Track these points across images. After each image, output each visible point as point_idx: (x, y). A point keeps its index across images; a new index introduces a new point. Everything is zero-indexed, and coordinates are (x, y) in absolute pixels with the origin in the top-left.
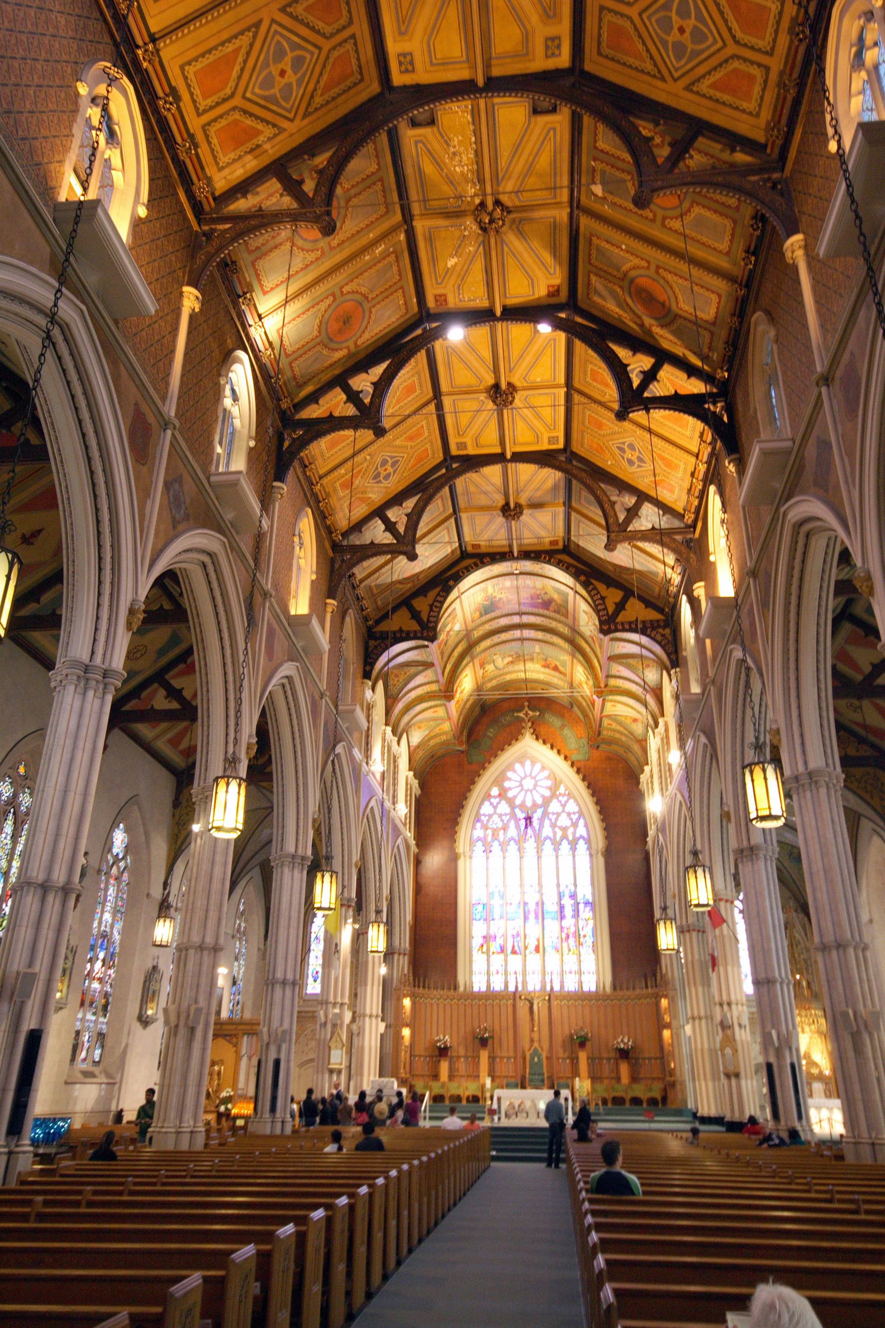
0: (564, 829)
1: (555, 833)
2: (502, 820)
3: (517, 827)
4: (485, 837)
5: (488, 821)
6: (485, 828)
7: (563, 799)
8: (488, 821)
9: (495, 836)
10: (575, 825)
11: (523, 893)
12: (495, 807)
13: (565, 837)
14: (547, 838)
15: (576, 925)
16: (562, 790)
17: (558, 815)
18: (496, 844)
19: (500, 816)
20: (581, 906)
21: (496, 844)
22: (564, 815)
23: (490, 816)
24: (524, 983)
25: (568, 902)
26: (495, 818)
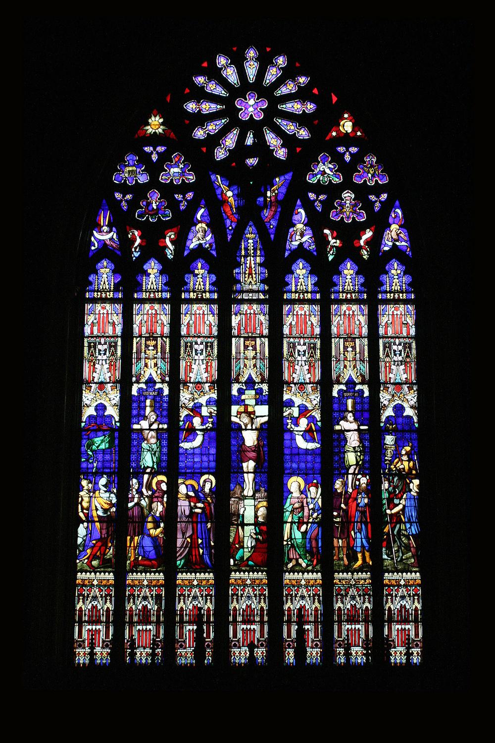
0: (349, 232)
1: (321, 241)
2: (174, 205)
3: (216, 224)
4: (126, 243)
5: (134, 205)
6: (121, 223)
7: (348, 153)
8: (134, 205)
9: (153, 250)
10: (380, 223)
11: (224, 402)
12: (154, 169)
13: (348, 252)
14: (301, 252)
15: (373, 490)
16: (347, 126)
17: (333, 192)
18: (153, 268)
19: (168, 191)
20: (389, 440)
21: (153, 268)
22: (348, 196)
23: (140, 191)
24: (223, 644)
25: (348, 425)
26: (155, 200)
